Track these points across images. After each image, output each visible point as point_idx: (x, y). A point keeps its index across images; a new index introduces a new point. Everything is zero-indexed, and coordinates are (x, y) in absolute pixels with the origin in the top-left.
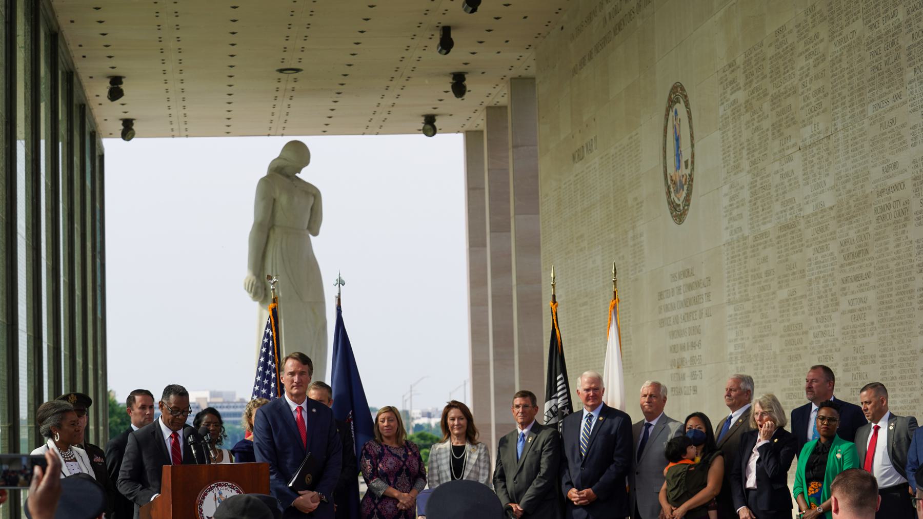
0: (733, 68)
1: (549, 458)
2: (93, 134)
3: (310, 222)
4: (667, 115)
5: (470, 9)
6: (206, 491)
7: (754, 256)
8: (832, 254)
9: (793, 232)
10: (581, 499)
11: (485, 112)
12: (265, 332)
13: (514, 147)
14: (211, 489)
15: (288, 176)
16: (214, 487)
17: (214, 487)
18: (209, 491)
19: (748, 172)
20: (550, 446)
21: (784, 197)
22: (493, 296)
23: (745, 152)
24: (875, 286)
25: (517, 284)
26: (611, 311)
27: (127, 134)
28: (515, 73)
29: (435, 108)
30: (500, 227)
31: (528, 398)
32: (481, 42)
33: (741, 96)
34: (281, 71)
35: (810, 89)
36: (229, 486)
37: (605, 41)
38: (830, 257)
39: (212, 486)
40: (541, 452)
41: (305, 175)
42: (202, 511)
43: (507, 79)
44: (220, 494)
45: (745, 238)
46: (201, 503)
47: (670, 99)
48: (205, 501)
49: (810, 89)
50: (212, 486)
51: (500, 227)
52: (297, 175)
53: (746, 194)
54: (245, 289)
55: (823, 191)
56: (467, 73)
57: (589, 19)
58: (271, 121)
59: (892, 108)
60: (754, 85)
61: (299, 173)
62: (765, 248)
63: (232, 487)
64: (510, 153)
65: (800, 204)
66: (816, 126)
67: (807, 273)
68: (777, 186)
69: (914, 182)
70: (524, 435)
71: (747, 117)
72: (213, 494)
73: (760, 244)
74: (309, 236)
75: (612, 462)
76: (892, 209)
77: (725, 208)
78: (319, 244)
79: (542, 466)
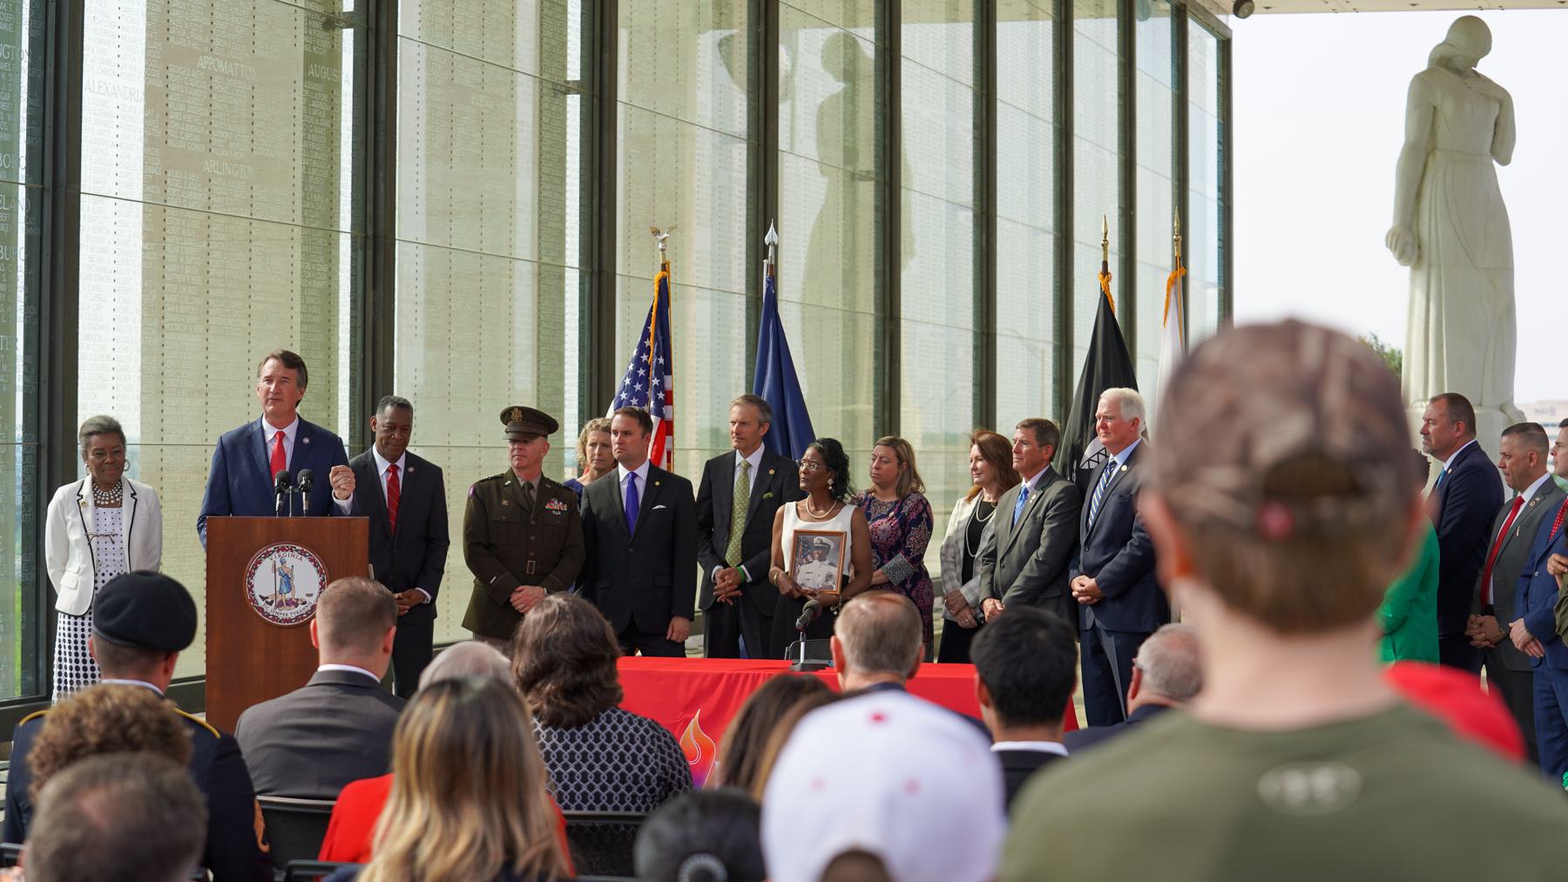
1: (1051, 529)
2: (1183, 8)
3: (1493, 142)
14: (268, 554)
15: (1458, 72)
16: (273, 551)
18: (265, 558)
20: (1055, 510)
26: (1168, 290)
27: (1242, 8)
31: (1035, 428)
36: (297, 550)
39: (270, 550)
40: (1044, 521)
41: (1484, 67)
44: (283, 563)
46: (252, 575)
48: (258, 572)
50: (270, 550)
54: (1387, 246)
63: (302, 553)
70: (1026, 492)
72: (272, 562)
74: (1493, 167)
75: (1131, 538)
79: (1041, 542)
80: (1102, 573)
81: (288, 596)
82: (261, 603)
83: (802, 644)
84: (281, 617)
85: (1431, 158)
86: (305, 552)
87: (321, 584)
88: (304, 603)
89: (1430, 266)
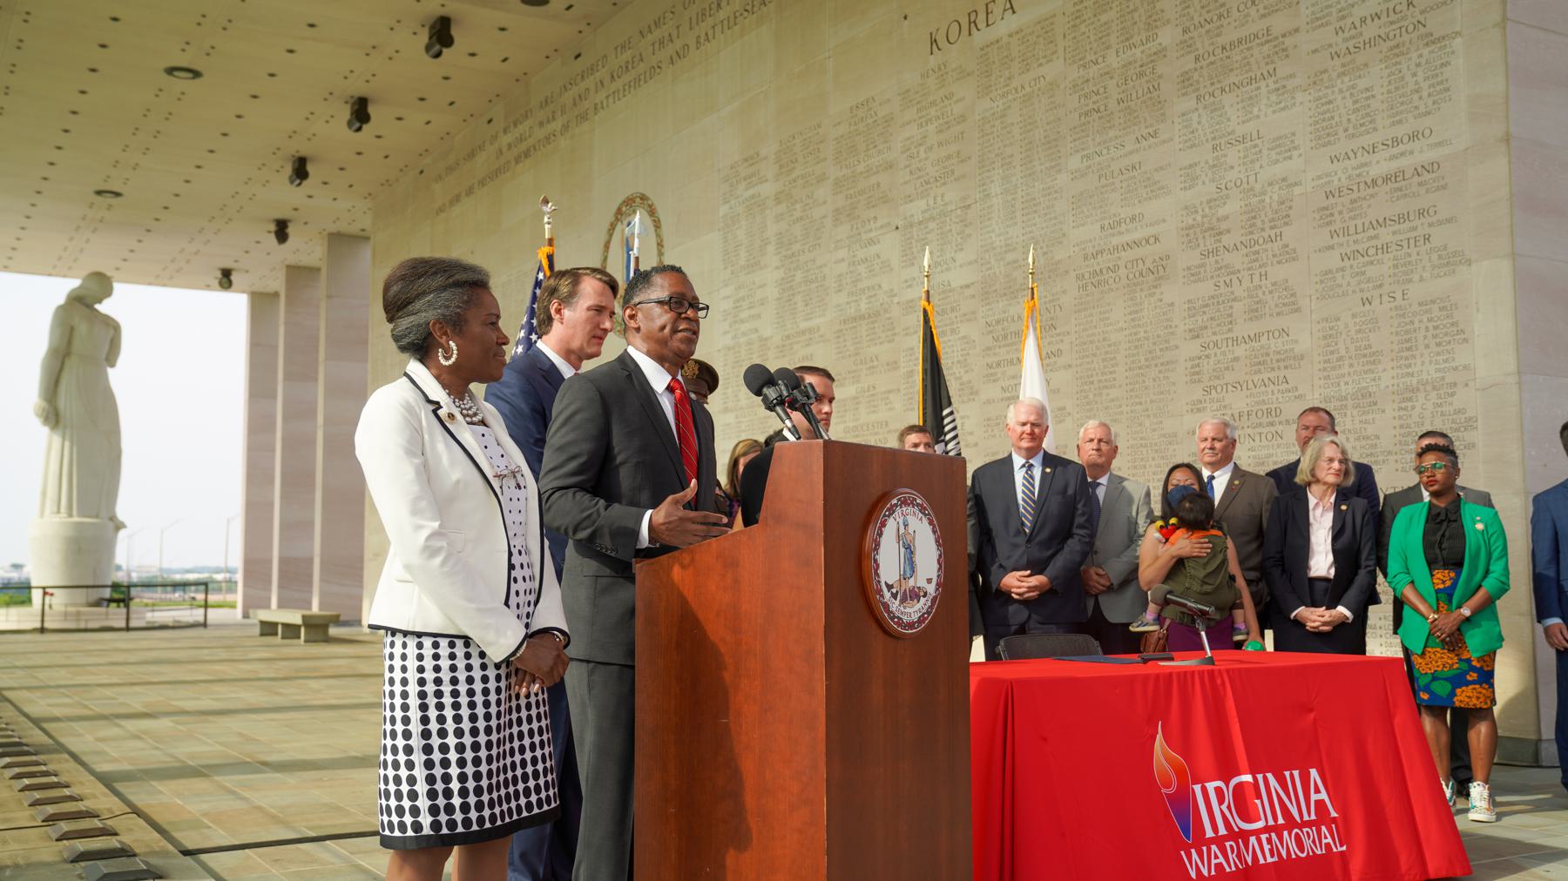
0: (751, 162)
4: (613, 227)
5: (358, 125)
6: (885, 515)
7: (784, 356)
8: (964, 337)
9: (873, 323)
10: (1031, 589)
11: (284, 270)
12: (534, 294)
13: (329, 297)
14: (892, 511)
17: (896, 505)
18: (889, 516)
19: (777, 268)
20: (970, 508)
21: (856, 286)
22: (284, 440)
23: (771, 249)
24: (1070, 366)
25: (325, 424)
28: (333, 228)
29: (236, 261)
30: (302, 372)
32: (325, 183)
33: (768, 189)
34: (99, 193)
35: (927, 159)
36: (918, 505)
37: (497, 173)
38: (959, 342)
41: (104, 307)
42: (878, 566)
43: (325, 233)
44: (906, 525)
45: (763, 340)
46: (878, 545)
47: (619, 212)
49: (927, 159)
51: (302, 372)
52: (97, 306)
53: (772, 292)
55: (948, 269)
56: (290, 221)
57: (471, 155)
58: (60, 258)
59: (1131, 153)
60: (797, 173)
61: (100, 301)
62: (808, 345)
64: (323, 304)
65: (892, 290)
66: (939, 199)
67: (903, 365)
68: (840, 276)
69: (1184, 233)
71: (782, 208)
73: (799, 342)
76: (1123, 272)
77: (725, 311)
78: (116, 377)
80: (1058, 563)
81: (911, 582)
82: (887, 595)
83: (1203, 633)
84: (905, 619)
85: (67, 360)
86: (925, 509)
87: (938, 561)
88: (924, 596)
89: (65, 427)
